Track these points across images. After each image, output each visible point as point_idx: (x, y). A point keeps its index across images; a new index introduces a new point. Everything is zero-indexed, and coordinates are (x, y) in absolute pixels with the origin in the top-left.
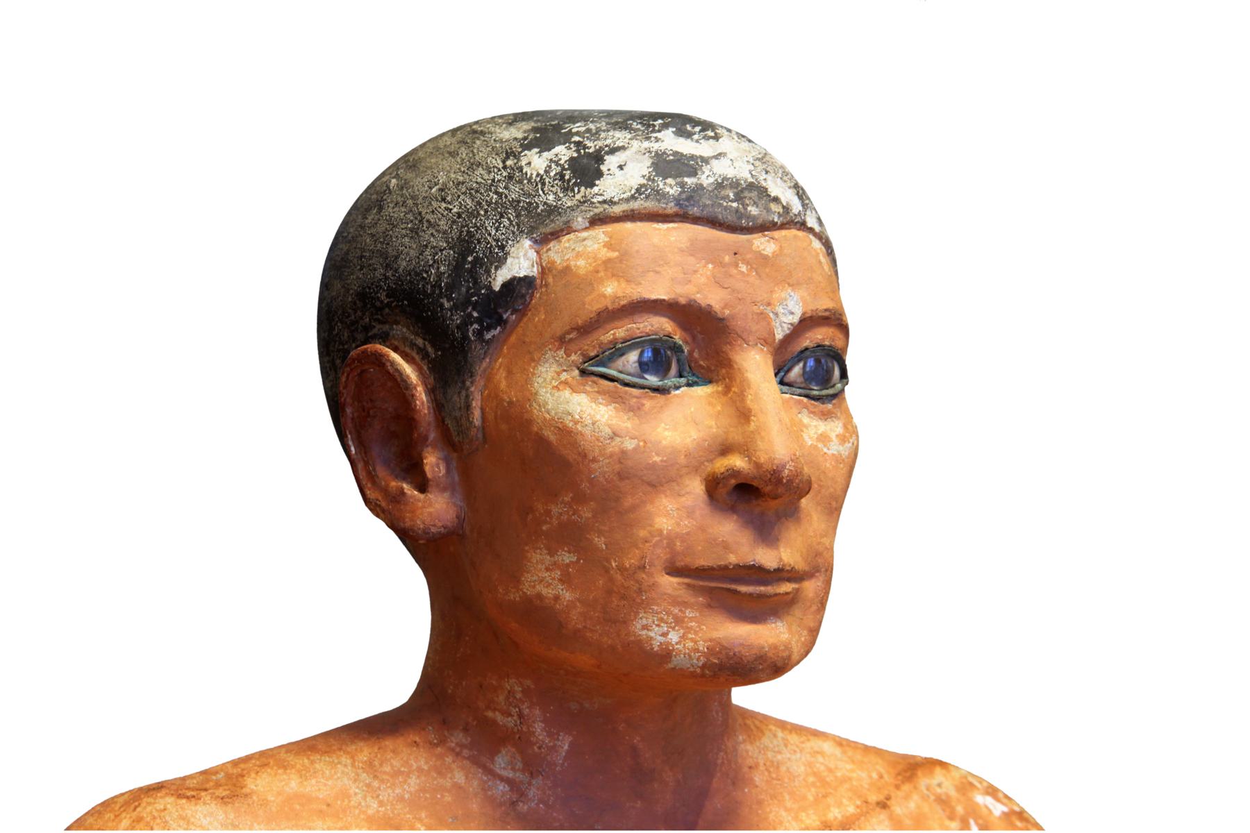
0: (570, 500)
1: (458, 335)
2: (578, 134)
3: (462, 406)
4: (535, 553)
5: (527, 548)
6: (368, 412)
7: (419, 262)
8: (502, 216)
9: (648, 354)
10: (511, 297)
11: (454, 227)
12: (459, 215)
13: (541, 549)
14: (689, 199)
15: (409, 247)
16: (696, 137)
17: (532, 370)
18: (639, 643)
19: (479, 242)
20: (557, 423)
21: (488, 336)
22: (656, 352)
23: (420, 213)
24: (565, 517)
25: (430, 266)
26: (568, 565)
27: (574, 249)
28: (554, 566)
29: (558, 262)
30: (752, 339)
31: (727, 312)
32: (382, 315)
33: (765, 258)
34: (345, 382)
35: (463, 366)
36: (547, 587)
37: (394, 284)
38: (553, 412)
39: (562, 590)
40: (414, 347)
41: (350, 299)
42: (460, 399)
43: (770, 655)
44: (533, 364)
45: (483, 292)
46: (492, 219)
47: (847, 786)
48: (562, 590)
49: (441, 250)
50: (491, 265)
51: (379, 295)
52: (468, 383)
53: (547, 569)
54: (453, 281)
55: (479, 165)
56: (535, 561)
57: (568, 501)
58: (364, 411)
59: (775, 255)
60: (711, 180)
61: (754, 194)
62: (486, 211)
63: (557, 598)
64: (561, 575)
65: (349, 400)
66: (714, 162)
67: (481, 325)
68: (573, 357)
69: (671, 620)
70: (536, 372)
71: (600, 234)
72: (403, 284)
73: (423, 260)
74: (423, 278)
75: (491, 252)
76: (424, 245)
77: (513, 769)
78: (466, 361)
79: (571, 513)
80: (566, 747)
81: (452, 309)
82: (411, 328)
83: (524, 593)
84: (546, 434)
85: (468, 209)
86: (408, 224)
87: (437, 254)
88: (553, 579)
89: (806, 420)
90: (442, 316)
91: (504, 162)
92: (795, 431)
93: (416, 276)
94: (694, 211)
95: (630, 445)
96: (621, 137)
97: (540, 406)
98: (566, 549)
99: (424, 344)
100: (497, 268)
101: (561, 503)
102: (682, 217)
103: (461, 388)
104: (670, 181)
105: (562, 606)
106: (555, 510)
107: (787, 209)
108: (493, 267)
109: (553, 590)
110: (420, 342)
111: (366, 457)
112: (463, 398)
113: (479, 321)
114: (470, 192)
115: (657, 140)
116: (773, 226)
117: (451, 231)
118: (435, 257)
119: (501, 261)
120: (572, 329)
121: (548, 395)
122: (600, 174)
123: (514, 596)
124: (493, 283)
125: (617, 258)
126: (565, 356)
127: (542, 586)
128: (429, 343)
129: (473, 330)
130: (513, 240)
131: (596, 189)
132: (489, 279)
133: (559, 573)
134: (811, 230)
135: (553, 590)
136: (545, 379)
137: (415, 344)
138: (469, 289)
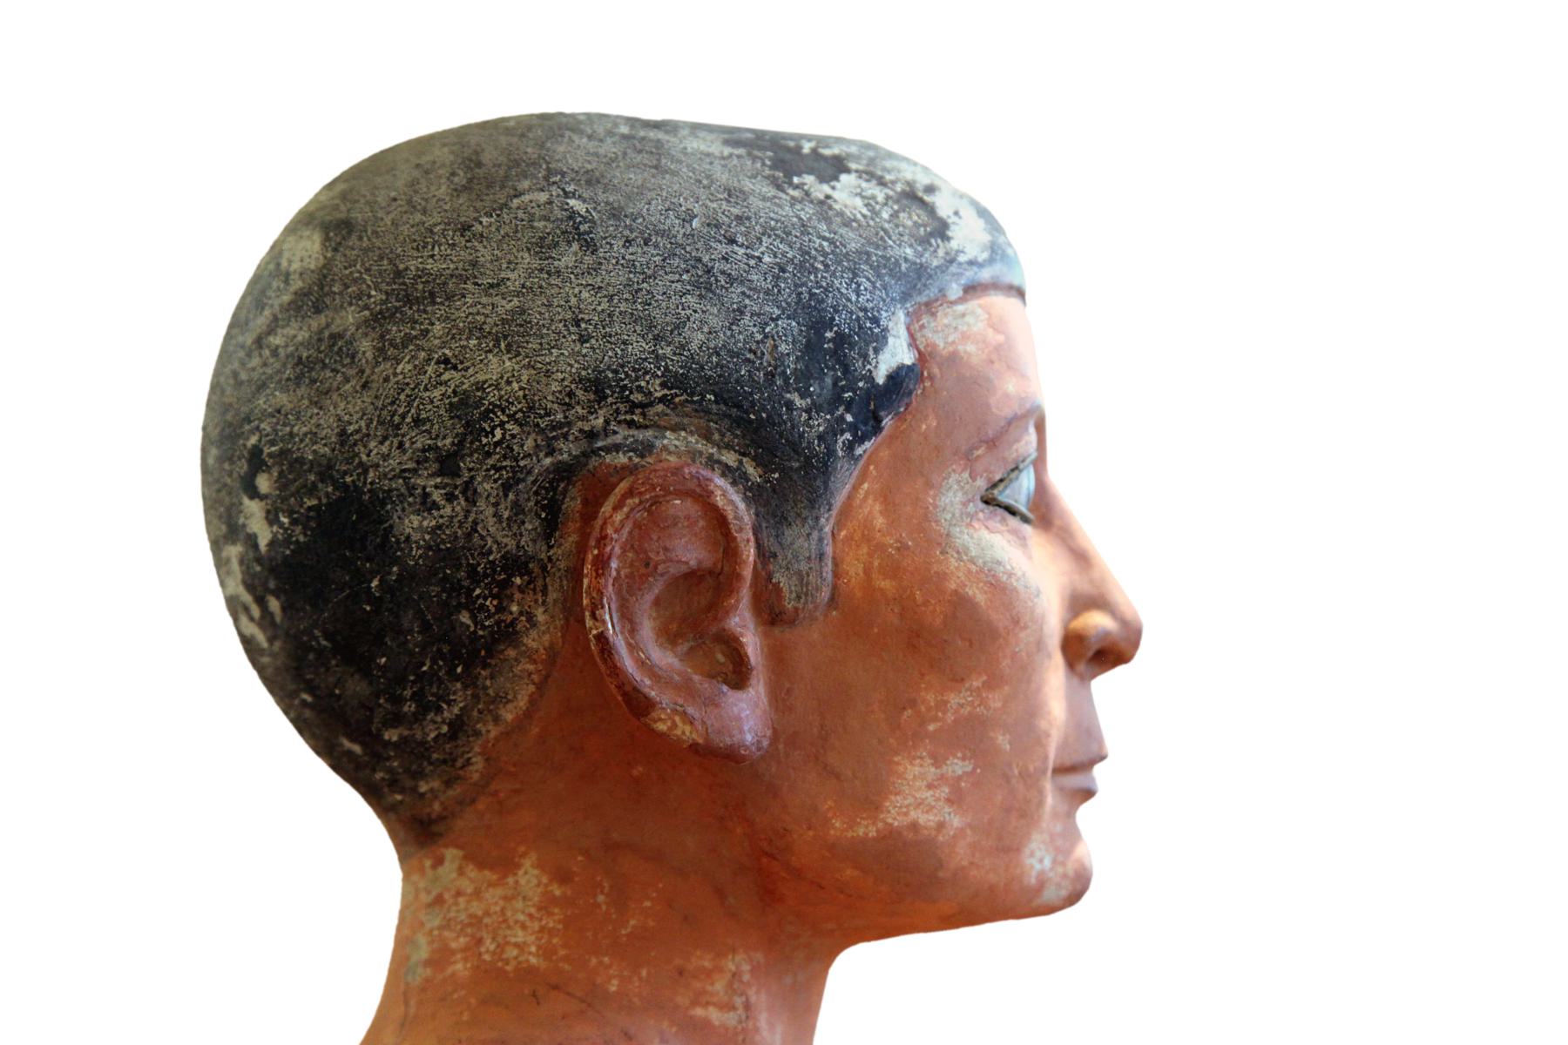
0: (980, 685)
3: (813, 556)
4: (911, 764)
5: (896, 759)
6: (656, 568)
7: (732, 336)
8: (855, 275)
10: (898, 395)
11: (783, 285)
13: (922, 758)
15: (703, 311)
17: (931, 501)
19: (836, 311)
20: (987, 576)
23: (699, 260)
24: (966, 711)
25: (758, 342)
26: (959, 778)
27: (956, 328)
28: (940, 782)
29: (942, 345)
32: (644, 415)
34: (621, 521)
35: (821, 495)
36: (927, 812)
37: (681, 367)
38: (981, 561)
39: (950, 814)
40: (716, 466)
41: (555, 387)
42: (809, 544)
44: (932, 493)
45: (861, 384)
46: (842, 277)
48: (950, 814)
49: (773, 320)
50: (867, 345)
51: (643, 384)
52: (823, 520)
53: (930, 786)
54: (806, 366)
56: (911, 777)
57: (978, 688)
58: (647, 565)
62: (827, 266)
64: (950, 793)
65: (617, 550)
67: (855, 435)
70: (938, 503)
72: (702, 368)
73: (740, 333)
74: (748, 360)
75: (860, 327)
76: (734, 311)
78: (826, 488)
79: (976, 703)
81: (811, 409)
82: (716, 437)
83: (886, 823)
84: (970, 593)
85: (792, 260)
86: (681, 275)
87: (767, 324)
88: (938, 799)
90: (791, 420)
93: (732, 357)
97: (958, 552)
98: (959, 755)
99: (741, 462)
100: (876, 351)
101: (967, 690)
103: (812, 528)
105: (947, 837)
106: (954, 699)
108: (871, 349)
109: (936, 815)
110: (730, 458)
111: (633, 638)
112: (814, 543)
113: (853, 428)
117: (779, 291)
118: (764, 329)
119: (880, 340)
120: (981, 441)
121: (966, 537)
123: (866, 829)
124: (874, 374)
126: (970, 481)
127: (920, 811)
128: (753, 459)
129: (843, 442)
130: (886, 311)
132: (868, 367)
133: (947, 791)
135: (936, 815)
136: (954, 515)
137: (719, 462)
138: (836, 381)
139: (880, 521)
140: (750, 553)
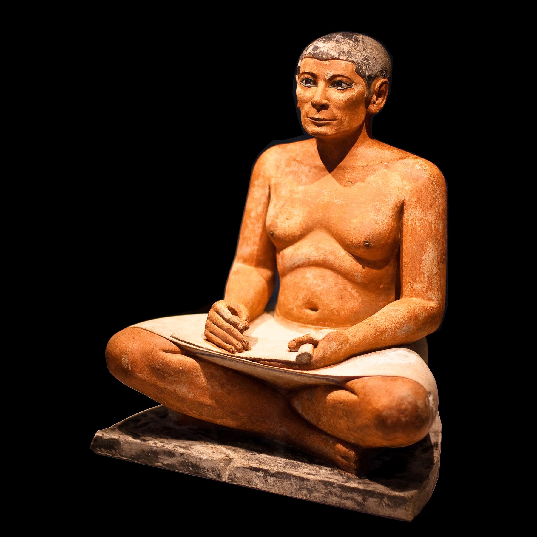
14: (314, 54)
33: (326, 65)
59: (329, 65)
95: (302, 96)
116: (329, 60)
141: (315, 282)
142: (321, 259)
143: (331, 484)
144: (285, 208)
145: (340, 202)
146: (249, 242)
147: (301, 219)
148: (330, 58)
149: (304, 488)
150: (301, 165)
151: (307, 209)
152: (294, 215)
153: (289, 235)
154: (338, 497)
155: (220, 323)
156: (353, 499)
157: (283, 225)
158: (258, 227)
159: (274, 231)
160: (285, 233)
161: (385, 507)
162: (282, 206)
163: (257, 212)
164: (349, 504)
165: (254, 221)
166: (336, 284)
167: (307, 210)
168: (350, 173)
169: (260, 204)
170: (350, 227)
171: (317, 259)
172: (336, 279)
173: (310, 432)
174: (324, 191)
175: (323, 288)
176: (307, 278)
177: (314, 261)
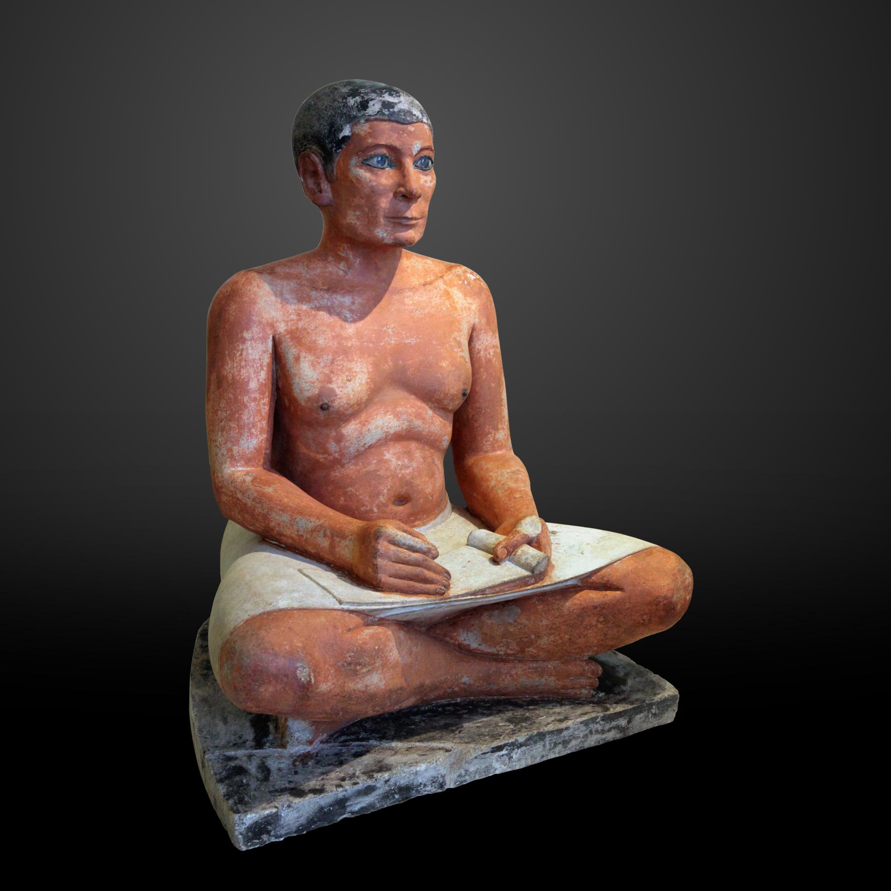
1: (330, 151)
2: (362, 93)
9: (380, 159)
12: (330, 116)
16: (394, 96)
18: (376, 237)
21: (338, 151)
22: (382, 158)
24: (358, 203)
30: (407, 155)
31: (400, 148)
33: (411, 132)
43: (409, 240)
47: (433, 272)
55: (336, 101)
59: (414, 131)
60: (397, 110)
61: (409, 114)
63: (355, 224)
65: (301, 166)
66: (398, 104)
68: (360, 159)
69: (384, 230)
71: (367, 125)
77: (345, 267)
80: (358, 262)
89: (421, 176)
91: (343, 100)
92: (419, 179)
94: (393, 119)
95: (374, 184)
96: (373, 96)
102: (390, 120)
104: (386, 110)
107: (418, 118)
110: (320, 151)
114: (334, 109)
115: (384, 97)
116: (414, 123)
119: (342, 130)
122: (368, 107)
125: (372, 132)
131: (367, 112)
134: (425, 123)
139: (342, 165)
140: (320, 168)
141: (399, 463)
142: (405, 427)
143: (594, 720)
144: (339, 365)
145: (413, 340)
146: (253, 430)
147: (366, 376)
148: (414, 121)
149: (559, 743)
150: (334, 296)
151: (371, 359)
152: (356, 372)
153: (354, 404)
154: (599, 733)
155: (407, 556)
156: (617, 727)
157: (346, 391)
158: (264, 404)
159: (330, 404)
160: (348, 402)
161: (650, 719)
162: (332, 362)
163: (258, 380)
164: (611, 736)
165: (257, 395)
166: (424, 458)
167: (371, 362)
168: (411, 298)
169: (261, 366)
170: (441, 374)
171: (398, 430)
172: (423, 452)
173: (507, 667)
174: (385, 329)
175: (413, 470)
176: (386, 461)
177: (395, 433)
